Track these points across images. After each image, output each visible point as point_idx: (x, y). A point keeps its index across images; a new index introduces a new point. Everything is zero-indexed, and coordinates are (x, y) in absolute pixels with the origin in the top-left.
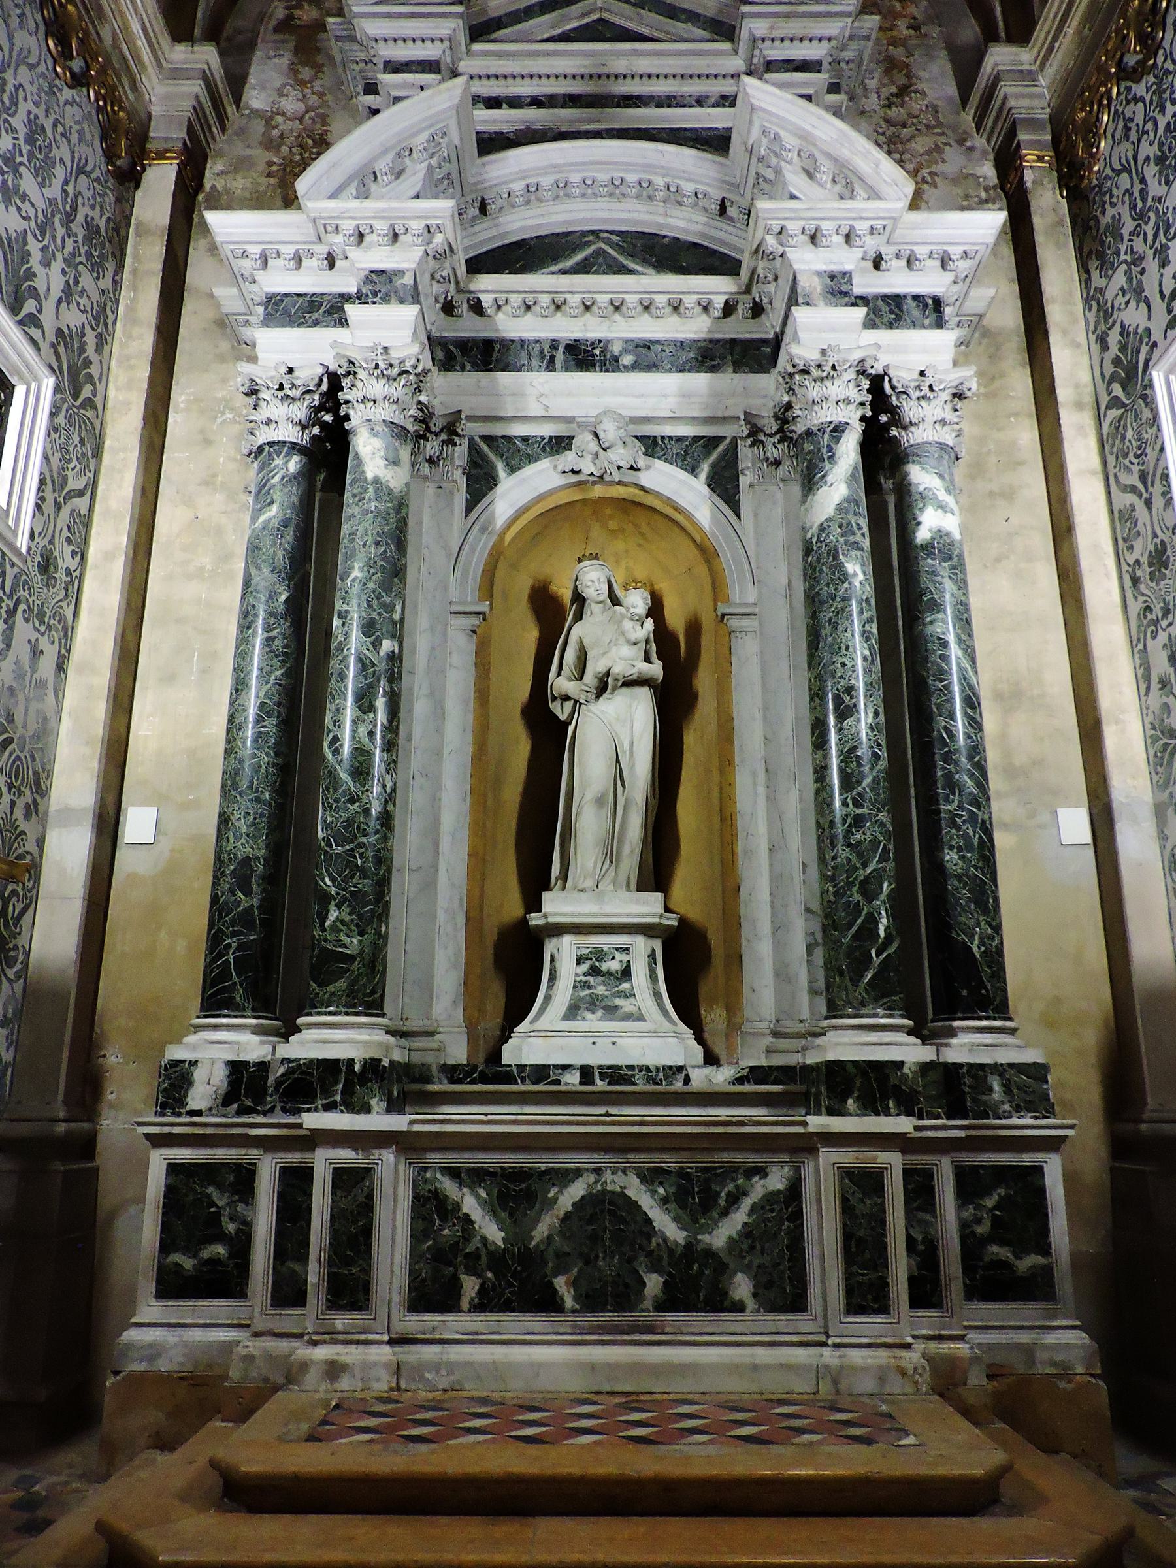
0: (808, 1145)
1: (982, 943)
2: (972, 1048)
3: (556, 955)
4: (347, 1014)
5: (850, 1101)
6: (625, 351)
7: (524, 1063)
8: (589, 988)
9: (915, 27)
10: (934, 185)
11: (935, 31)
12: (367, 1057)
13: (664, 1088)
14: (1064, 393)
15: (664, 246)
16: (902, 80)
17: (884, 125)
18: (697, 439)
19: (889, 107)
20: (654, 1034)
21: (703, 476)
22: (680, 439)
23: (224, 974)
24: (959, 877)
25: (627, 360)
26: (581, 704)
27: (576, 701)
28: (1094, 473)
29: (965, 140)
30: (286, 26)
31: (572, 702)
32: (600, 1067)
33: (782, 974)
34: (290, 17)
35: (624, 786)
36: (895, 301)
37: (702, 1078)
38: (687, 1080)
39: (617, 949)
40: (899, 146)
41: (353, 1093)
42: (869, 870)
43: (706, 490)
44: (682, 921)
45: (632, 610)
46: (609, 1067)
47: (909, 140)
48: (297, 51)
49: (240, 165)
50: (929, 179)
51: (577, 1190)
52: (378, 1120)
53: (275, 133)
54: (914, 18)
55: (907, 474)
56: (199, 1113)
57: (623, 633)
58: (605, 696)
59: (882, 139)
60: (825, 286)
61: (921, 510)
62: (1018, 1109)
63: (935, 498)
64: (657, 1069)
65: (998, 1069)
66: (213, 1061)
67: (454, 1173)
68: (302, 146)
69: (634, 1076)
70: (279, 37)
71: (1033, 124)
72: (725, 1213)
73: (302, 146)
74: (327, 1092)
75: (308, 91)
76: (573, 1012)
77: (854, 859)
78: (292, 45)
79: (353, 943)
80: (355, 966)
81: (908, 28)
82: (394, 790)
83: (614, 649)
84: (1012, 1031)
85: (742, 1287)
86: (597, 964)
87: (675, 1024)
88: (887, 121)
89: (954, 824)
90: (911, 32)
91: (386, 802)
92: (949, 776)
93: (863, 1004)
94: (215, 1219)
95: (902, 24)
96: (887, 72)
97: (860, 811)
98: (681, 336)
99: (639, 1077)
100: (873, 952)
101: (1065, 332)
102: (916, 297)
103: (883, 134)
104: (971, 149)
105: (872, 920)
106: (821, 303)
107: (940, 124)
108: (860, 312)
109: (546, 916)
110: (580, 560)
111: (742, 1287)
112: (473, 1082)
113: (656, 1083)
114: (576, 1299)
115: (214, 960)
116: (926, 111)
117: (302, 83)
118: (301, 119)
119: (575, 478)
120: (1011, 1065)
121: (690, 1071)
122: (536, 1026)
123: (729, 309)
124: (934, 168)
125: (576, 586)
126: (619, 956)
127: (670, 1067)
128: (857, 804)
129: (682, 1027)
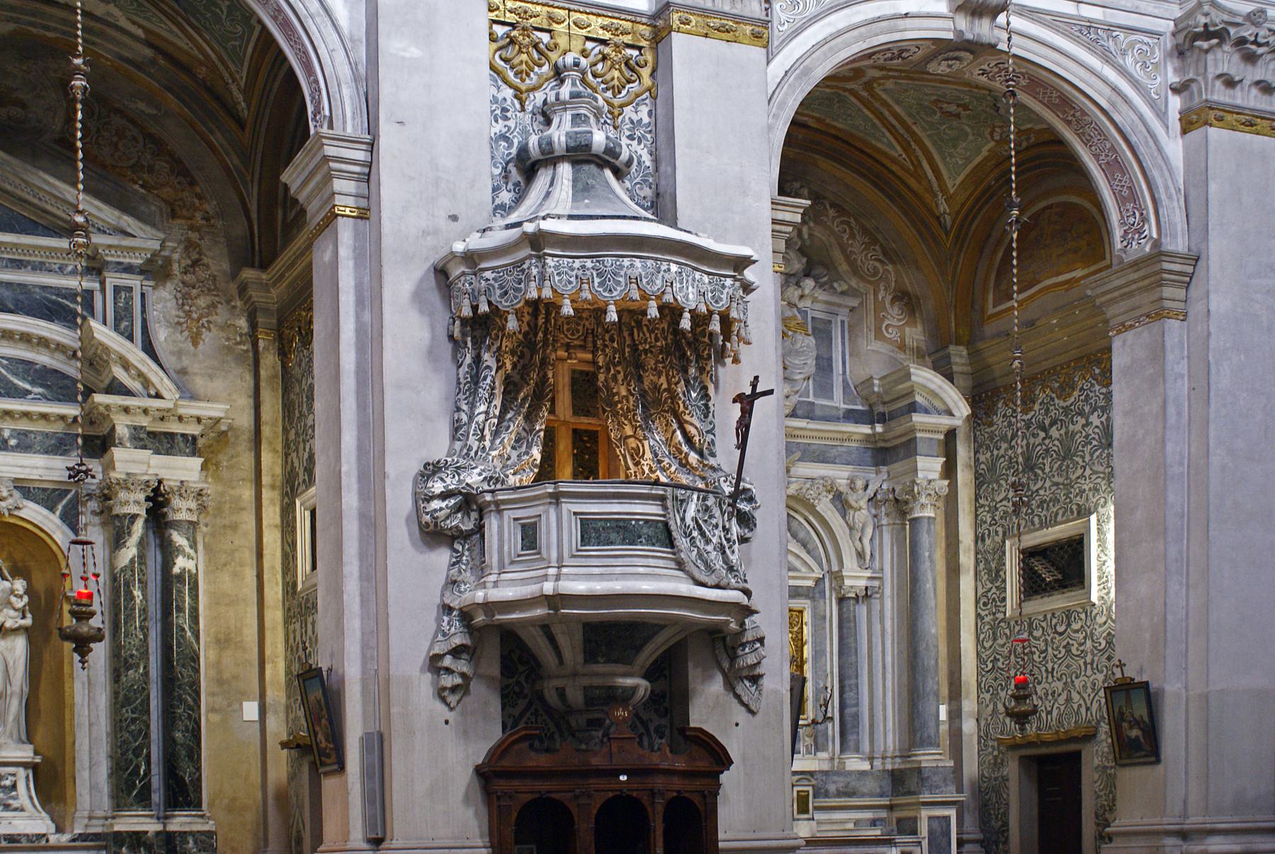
1: (190, 776)
2: (182, 824)
6: (12, 436)
9: (207, 220)
11: (219, 224)
13: (36, 844)
14: (266, 479)
16: (195, 256)
17: (181, 285)
18: (54, 490)
19: (186, 273)
22: (44, 490)
24: (182, 745)
25: (13, 442)
28: (276, 526)
37: (53, 839)
40: (190, 301)
59: (179, 295)
81: (202, 219)
84: (202, 816)
88: (183, 282)
90: (204, 222)
92: (180, 695)
93: (132, 805)
95: (198, 215)
96: (186, 248)
98: (47, 430)
99: (23, 840)
101: (270, 443)
105: (138, 767)
107: (216, 289)
116: (208, 279)
124: (210, 318)
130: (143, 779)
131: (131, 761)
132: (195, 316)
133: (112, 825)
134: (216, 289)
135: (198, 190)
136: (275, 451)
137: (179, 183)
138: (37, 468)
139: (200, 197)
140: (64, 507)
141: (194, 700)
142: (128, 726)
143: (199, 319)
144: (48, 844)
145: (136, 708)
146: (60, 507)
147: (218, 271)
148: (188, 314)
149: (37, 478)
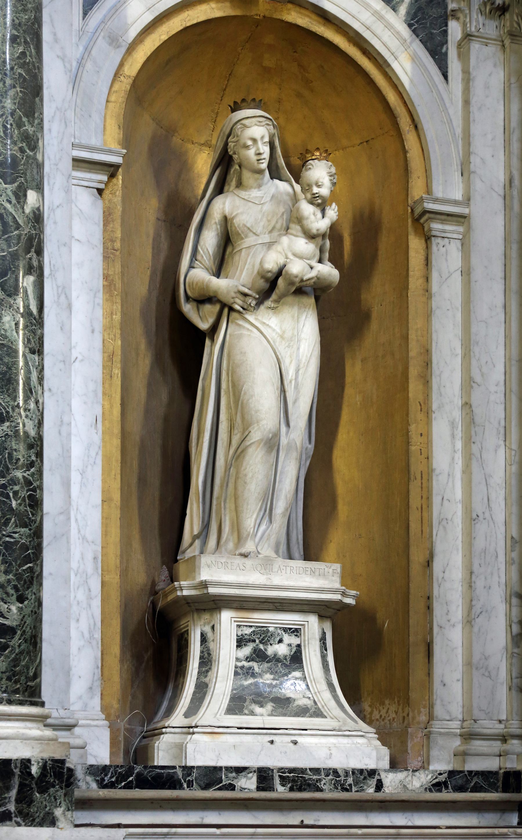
3: (210, 635)
7: (190, 763)
8: (253, 675)
13: (352, 795)
21: (403, 9)
26: (231, 309)
27: (223, 305)
31: (217, 307)
32: (281, 770)
35: (288, 425)
38: (379, 786)
39: (285, 630)
43: (405, 31)
46: (292, 770)
58: (269, 303)
69: (320, 780)
86: (261, 647)
87: (356, 722)
99: (326, 783)
110: (235, 108)
112: (128, 786)
113: (347, 790)
121: (383, 775)
122: (198, 719)
125: (226, 144)
126: (288, 639)
127: (361, 771)
144: (379, 796)
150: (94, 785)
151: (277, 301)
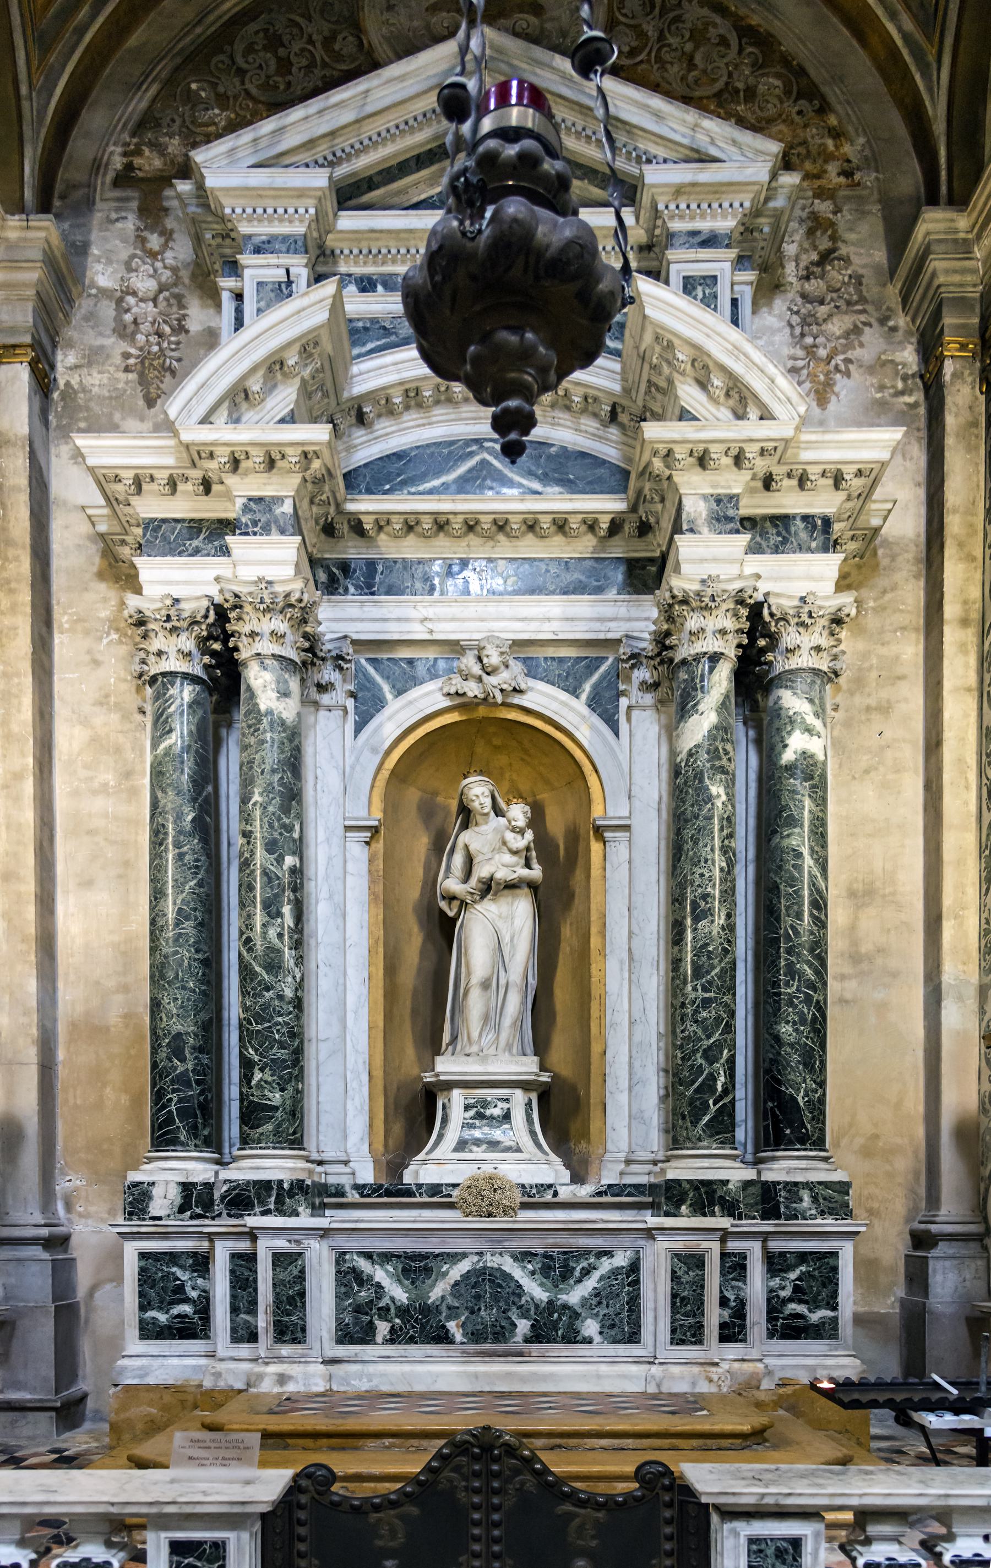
0: (649, 1234)
1: (806, 1095)
2: (789, 1171)
4: (274, 1148)
5: (683, 1207)
9: (848, 174)
10: (848, 374)
11: (868, 178)
12: (294, 1178)
14: (951, 610)
15: (550, 457)
16: (825, 244)
17: (799, 300)
19: (807, 278)
20: (529, 1161)
23: (169, 1120)
24: (791, 1045)
29: (887, 318)
30: (125, 178)
33: (634, 1117)
34: (129, 167)
36: (782, 521)
37: (565, 1193)
38: (555, 1194)
40: (814, 328)
41: (284, 1203)
42: (711, 1041)
44: (556, 1077)
45: (513, 823)
47: (825, 320)
48: (143, 212)
49: (93, 358)
50: (842, 367)
51: (464, 1266)
52: (305, 1219)
53: (128, 317)
54: (849, 161)
55: (779, 698)
56: (160, 1218)
57: (504, 843)
58: (489, 896)
59: (796, 319)
60: (711, 511)
61: (789, 733)
62: (822, 1213)
63: (803, 721)
64: (531, 1187)
65: (808, 1185)
66: (167, 1183)
67: (368, 1256)
68: (160, 334)
70: (117, 193)
71: (961, 303)
72: (579, 1281)
73: (160, 334)
74: (262, 1202)
75: (159, 265)
76: (462, 1145)
77: (700, 1032)
78: (134, 204)
79: (276, 1098)
80: (279, 1114)
82: (302, 980)
83: (497, 857)
84: (826, 1159)
85: (590, 1327)
88: (804, 296)
89: (791, 1004)
90: (842, 180)
91: (297, 989)
92: (790, 966)
93: (700, 1139)
94: (180, 1289)
95: (832, 169)
97: (708, 995)
100: (711, 1102)
102: (806, 518)
103: (797, 313)
104: (894, 329)
105: (712, 1078)
106: (705, 530)
107: (862, 300)
108: (744, 539)
109: (437, 1075)
111: (590, 1327)
114: (465, 1335)
115: (160, 1110)
116: (849, 283)
117: (153, 255)
118: (155, 300)
119: (458, 701)
120: (820, 1183)
123: (615, 527)
124: (849, 355)
127: (542, 1185)
128: (705, 989)
129: (552, 1156)
130: (721, 1098)
131: (700, 1070)
132: (822, 353)
133: (663, 1171)
134: (862, 300)
135: (833, 120)
136: (971, 558)
137: (800, 113)
138: (549, 620)
139: (837, 134)
140: (595, 687)
141: (817, 972)
142: (696, 1012)
143: (829, 359)
144: (555, 1200)
145: (710, 983)
146: (587, 687)
147: (864, 266)
148: (810, 351)
149: (551, 636)
150: (357, 1196)
151: (495, 894)
